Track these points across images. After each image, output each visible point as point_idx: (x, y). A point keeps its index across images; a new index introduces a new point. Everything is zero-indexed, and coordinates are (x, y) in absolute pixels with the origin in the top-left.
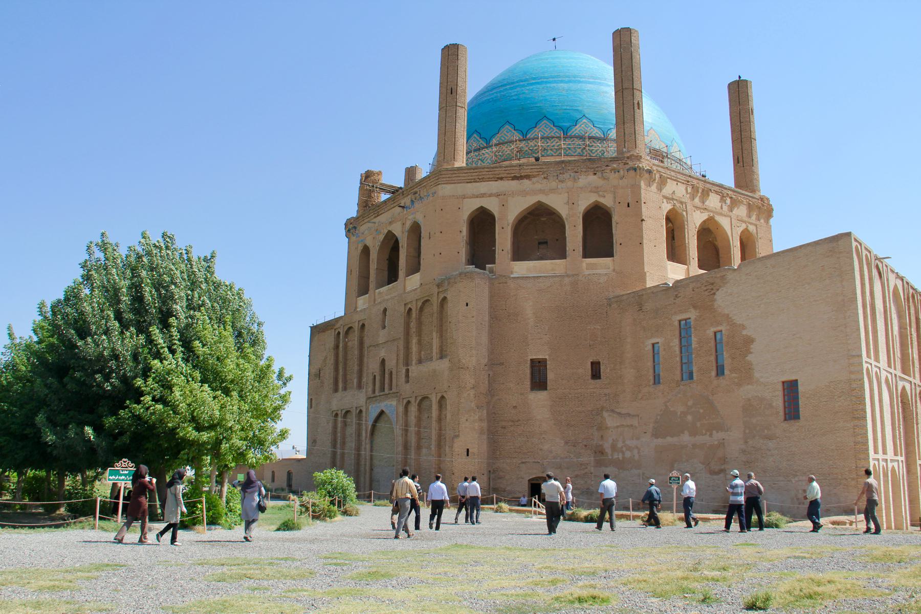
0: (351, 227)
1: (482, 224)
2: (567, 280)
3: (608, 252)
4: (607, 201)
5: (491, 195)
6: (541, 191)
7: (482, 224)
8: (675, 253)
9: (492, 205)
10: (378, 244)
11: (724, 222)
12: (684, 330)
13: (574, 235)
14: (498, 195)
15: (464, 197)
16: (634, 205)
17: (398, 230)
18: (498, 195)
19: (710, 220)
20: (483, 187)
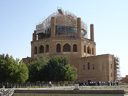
0: (32, 43)
1: (59, 46)
2: (71, 55)
3: (76, 51)
4: (77, 44)
5: (60, 42)
6: (67, 42)
7: (59, 46)
8: (85, 52)
9: (60, 43)
10: (39, 47)
11: (90, 46)
12: (89, 64)
13: (72, 48)
14: (61, 42)
15: (56, 42)
16: (80, 44)
17: (43, 45)
18: (61, 42)
19: (89, 46)
20: (59, 40)
